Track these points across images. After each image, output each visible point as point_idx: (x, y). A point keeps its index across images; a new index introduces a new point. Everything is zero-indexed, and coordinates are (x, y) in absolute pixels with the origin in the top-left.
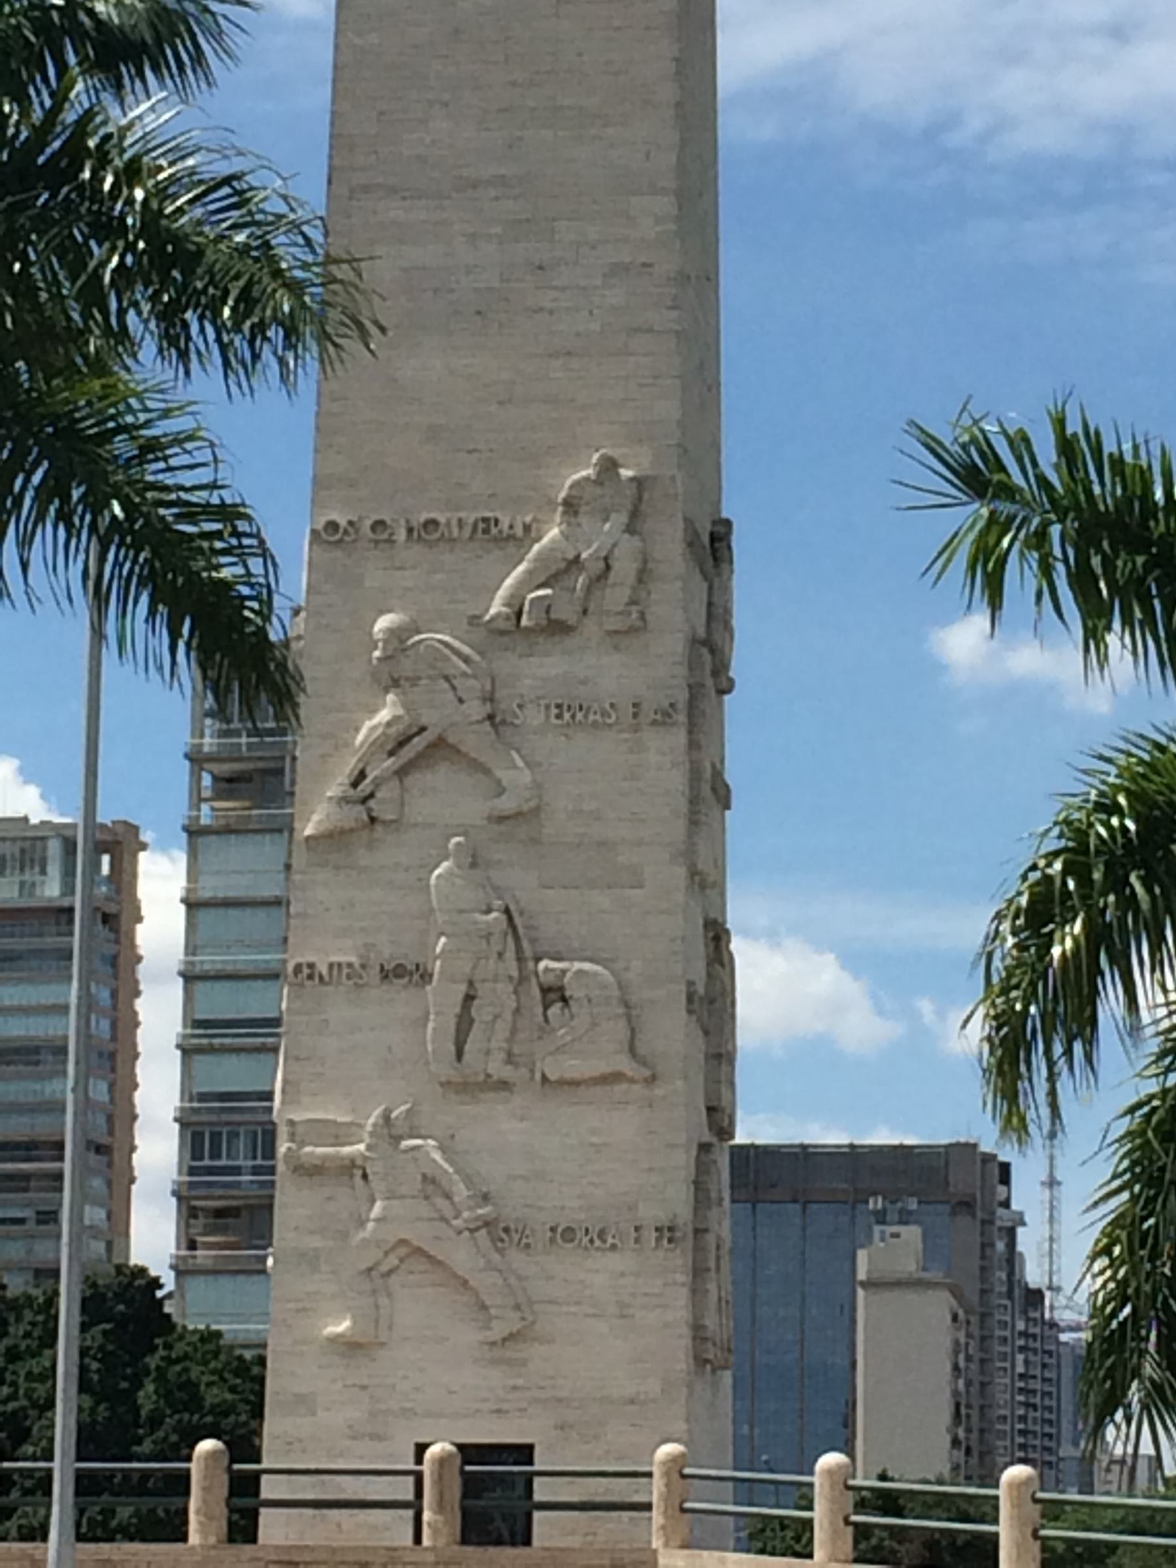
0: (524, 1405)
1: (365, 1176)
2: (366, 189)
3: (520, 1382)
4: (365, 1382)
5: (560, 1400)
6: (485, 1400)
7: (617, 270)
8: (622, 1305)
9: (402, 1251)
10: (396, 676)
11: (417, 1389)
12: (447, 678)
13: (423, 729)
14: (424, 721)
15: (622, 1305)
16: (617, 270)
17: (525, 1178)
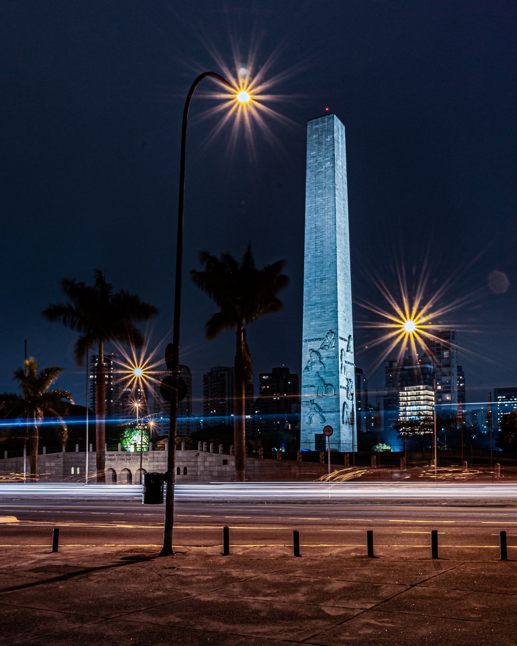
7: (331, 311)
16: (331, 311)
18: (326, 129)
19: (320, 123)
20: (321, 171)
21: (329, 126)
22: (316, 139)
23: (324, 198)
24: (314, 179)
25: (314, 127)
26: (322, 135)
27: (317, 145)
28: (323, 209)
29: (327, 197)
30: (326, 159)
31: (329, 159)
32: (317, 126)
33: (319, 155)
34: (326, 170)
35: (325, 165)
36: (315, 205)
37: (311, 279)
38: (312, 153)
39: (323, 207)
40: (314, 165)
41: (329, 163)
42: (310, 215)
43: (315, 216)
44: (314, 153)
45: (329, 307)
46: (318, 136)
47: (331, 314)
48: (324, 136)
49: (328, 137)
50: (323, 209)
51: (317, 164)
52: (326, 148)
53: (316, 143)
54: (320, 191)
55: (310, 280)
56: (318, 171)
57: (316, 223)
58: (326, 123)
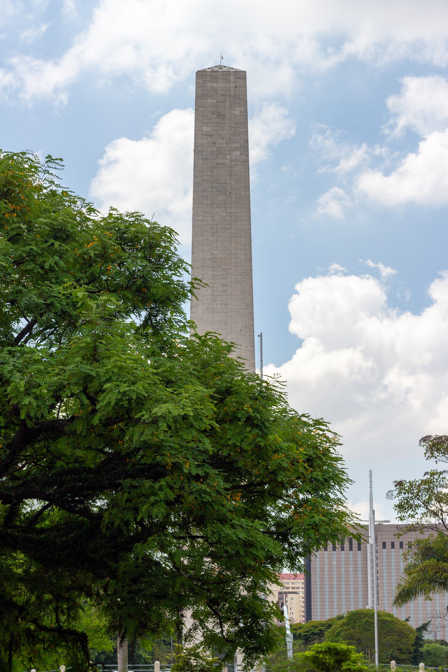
18: (232, 93)
19: (220, 80)
20: (223, 164)
21: (237, 89)
22: (213, 106)
23: (228, 211)
24: (209, 173)
25: (209, 85)
26: (224, 102)
27: (215, 116)
28: (227, 229)
29: (233, 211)
30: (233, 145)
31: (238, 145)
32: (215, 85)
33: (219, 135)
34: (233, 163)
35: (230, 154)
36: (211, 219)
38: (205, 129)
39: (228, 227)
40: (209, 149)
41: (238, 153)
42: (202, 235)
43: (211, 238)
44: (209, 129)
46: (217, 102)
48: (228, 104)
49: (237, 109)
50: (227, 229)
51: (215, 149)
52: (233, 125)
53: (213, 113)
56: (219, 161)
57: (213, 252)
58: (232, 85)
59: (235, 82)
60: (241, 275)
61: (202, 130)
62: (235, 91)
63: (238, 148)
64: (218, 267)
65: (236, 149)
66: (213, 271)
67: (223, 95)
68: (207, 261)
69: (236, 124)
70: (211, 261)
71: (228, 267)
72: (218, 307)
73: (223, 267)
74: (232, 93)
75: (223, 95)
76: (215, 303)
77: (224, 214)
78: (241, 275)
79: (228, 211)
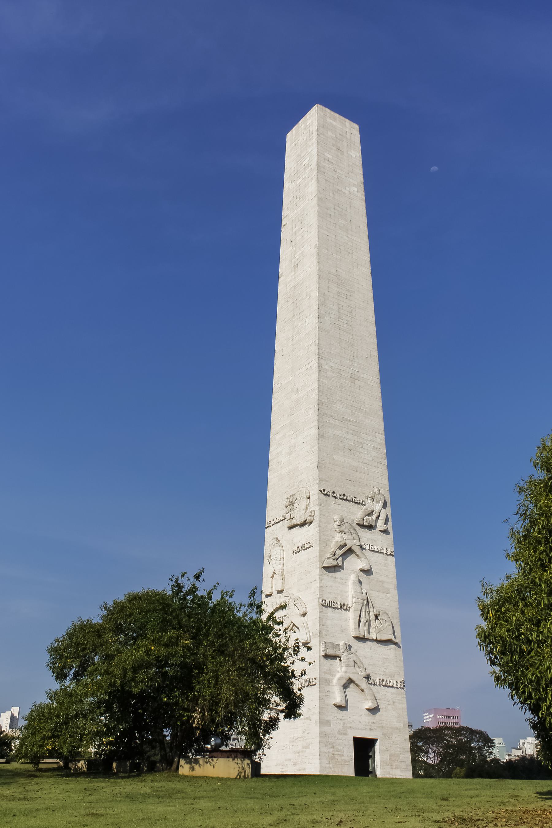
0: (375, 728)
1: (340, 660)
2: (326, 414)
3: (375, 721)
4: (341, 718)
5: (383, 727)
6: (367, 725)
7: (374, 448)
8: (394, 702)
9: (349, 681)
10: (341, 530)
11: (353, 721)
12: (351, 533)
13: (346, 545)
14: (347, 543)
15: (394, 702)
17: (372, 665)
20: (344, 193)
32: (333, 123)
36: (334, 237)
37: (331, 364)
39: (350, 251)
45: (369, 438)
47: (374, 454)
50: (349, 253)
51: (336, 177)
53: (333, 145)
54: (342, 222)
55: (331, 367)
59: (350, 130)
60: (364, 302)
61: (324, 155)
62: (351, 137)
63: (355, 185)
64: (342, 286)
65: (354, 185)
66: (338, 287)
67: (341, 135)
68: (333, 276)
69: (353, 164)
70: (336, 277)
71: (351, 290)
72: (344, 326)
73: (347, 288)
74: (348, 137)
75: (341, 135)
76: (340, 320)
77: (346, 238)
78: (364, 302)
79: (349, 236)
